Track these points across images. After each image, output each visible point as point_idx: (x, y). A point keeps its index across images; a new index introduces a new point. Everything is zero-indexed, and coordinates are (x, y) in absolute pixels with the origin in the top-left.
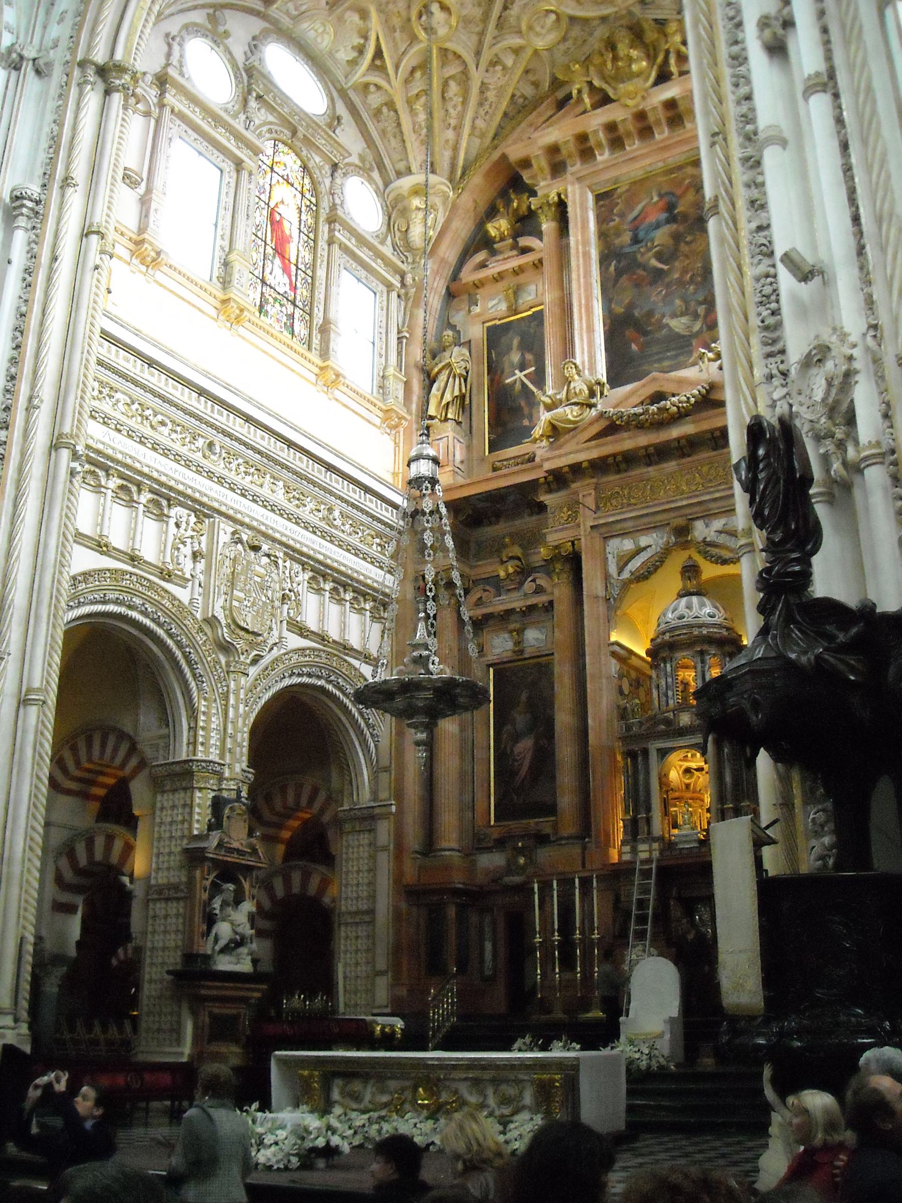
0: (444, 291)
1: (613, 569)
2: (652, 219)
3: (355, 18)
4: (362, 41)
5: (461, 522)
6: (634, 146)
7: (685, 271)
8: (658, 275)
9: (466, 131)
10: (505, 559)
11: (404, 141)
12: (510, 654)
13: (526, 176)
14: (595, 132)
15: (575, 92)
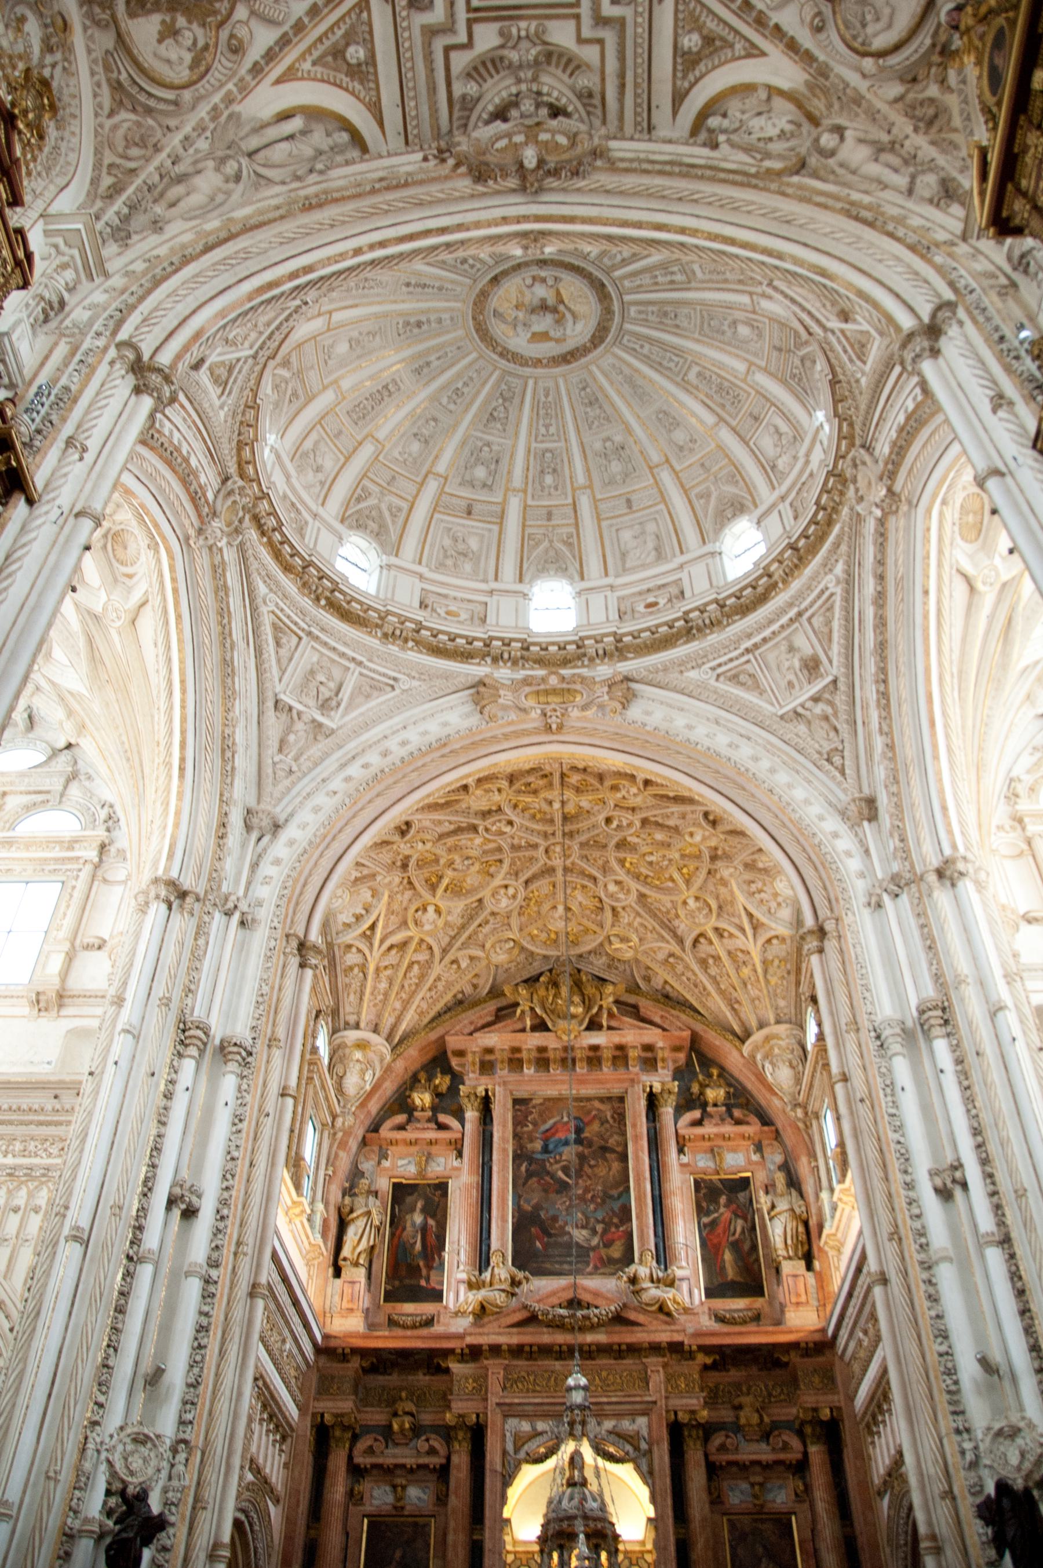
0: (360, 1138)
1: (510, 1447)
2: (561, 1135)
3: (369, 893)
4: (363, 912)
5: (363, 1368)
6: (555, 1071)
7: (587, 1190)
8: (563, 1187)
9: (414, 1007)
10: (400, 1413)
11: (361, 999)
12: (389, 1508)
13: (454, 1062)
14: (529, 1050)
15: (519, 1011)
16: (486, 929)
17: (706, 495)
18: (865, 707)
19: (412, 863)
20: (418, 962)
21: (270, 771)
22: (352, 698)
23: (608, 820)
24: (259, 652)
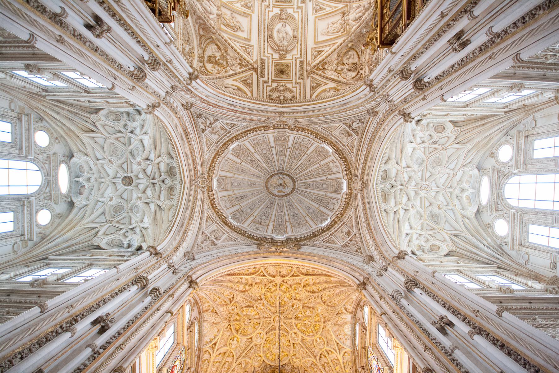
3: (217, 330)
16: (252, 351)
17: (317, 220)
18: (365, 237)
19: (232, 319)
20: (228, 362)
21: (196, 245)
22: (224, 240)
23: (292, 306)
24: (201, 219)
